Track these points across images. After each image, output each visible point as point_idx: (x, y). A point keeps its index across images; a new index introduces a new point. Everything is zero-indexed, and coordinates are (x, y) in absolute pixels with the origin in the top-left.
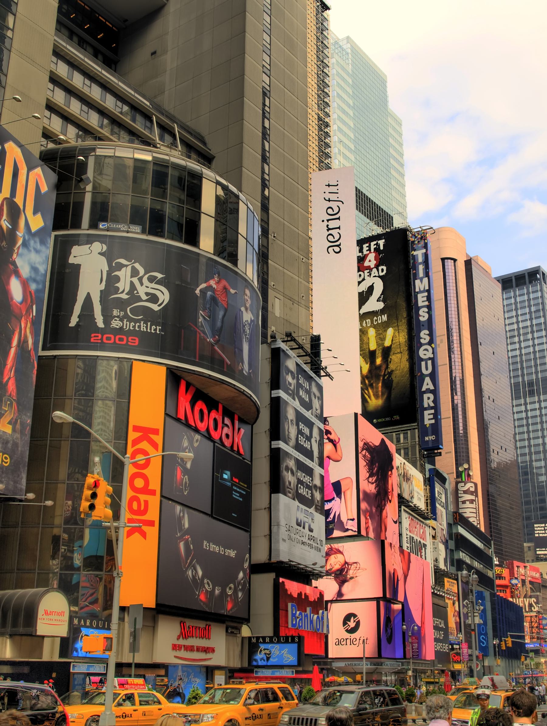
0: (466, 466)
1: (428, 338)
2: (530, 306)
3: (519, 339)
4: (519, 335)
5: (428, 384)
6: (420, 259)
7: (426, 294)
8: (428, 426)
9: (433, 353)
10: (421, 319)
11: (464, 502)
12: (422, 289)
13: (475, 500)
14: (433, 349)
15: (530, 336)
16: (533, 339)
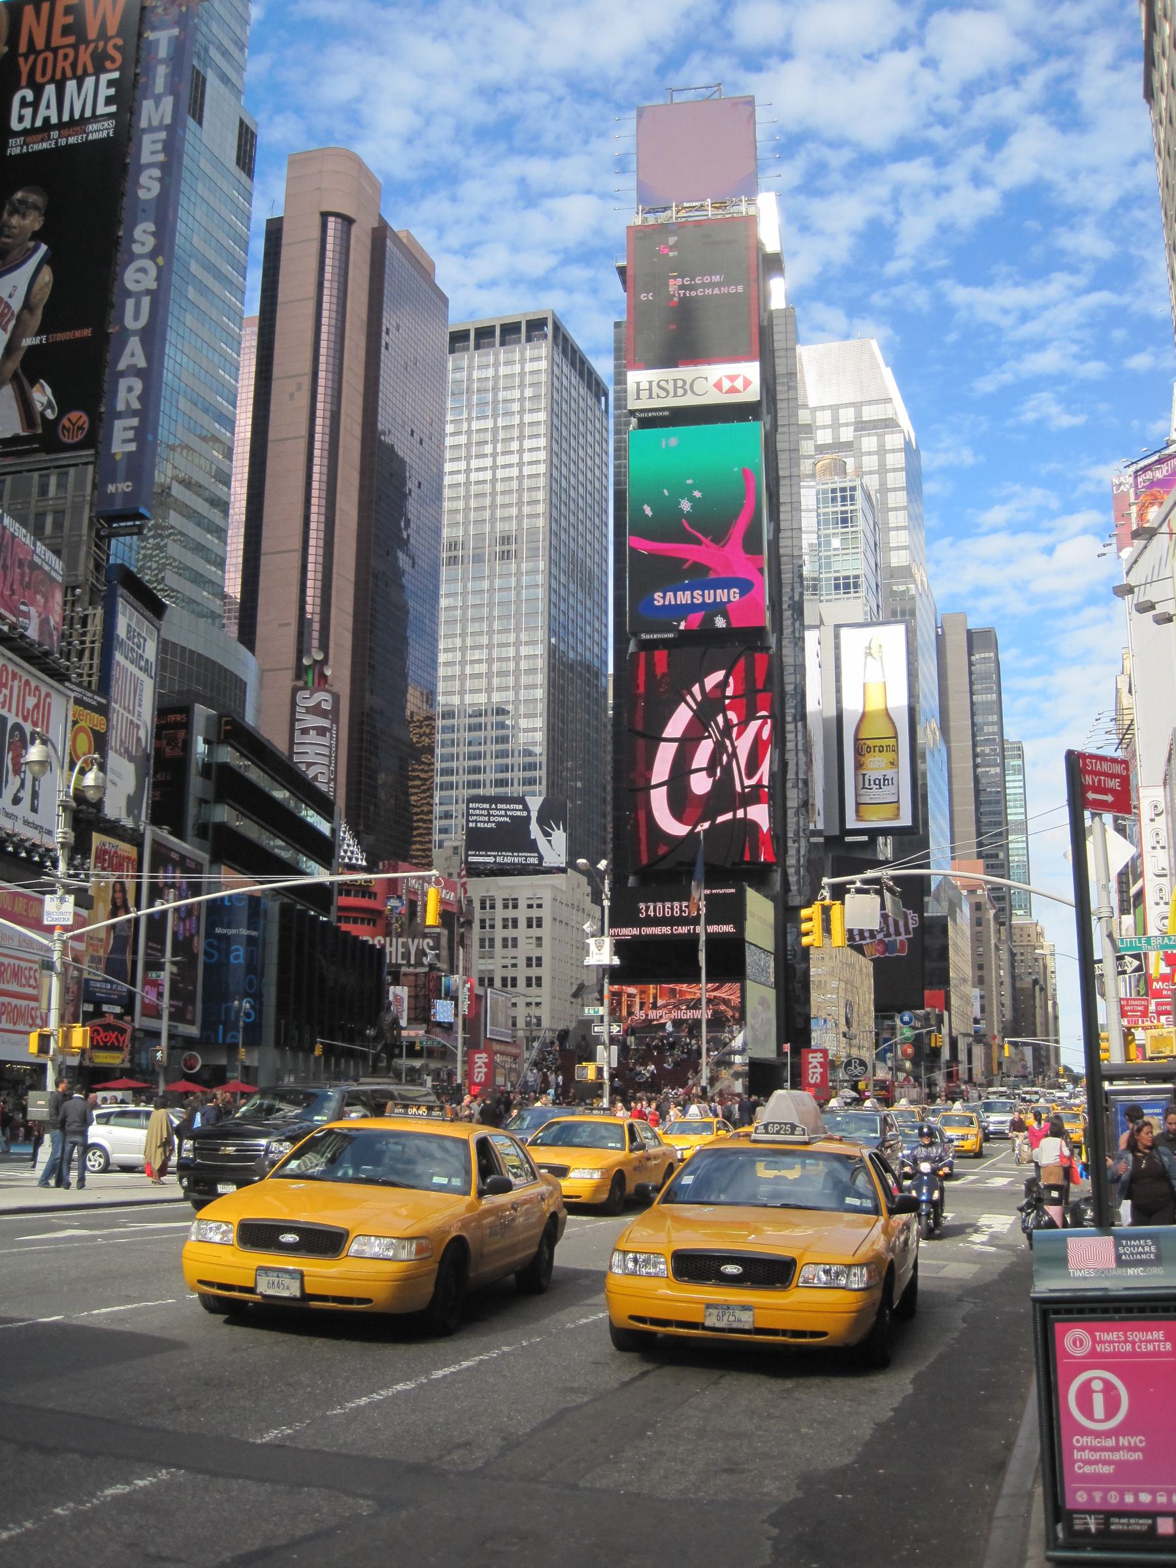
0: (319, 657)
1: (150, 242)
2: (522, 386)
3: (495, 448)
4: (495, 442)
5: (133, 355)
6: (163, 52)
7: (163, 135)
8: (118, 457)
9: (158, 278)
10: (142, 194)
11: (305, 731)
12: (155, 123)
13: (330, 730)
14: (160, 269)
15: (515, 446)
16: (521, 451)
